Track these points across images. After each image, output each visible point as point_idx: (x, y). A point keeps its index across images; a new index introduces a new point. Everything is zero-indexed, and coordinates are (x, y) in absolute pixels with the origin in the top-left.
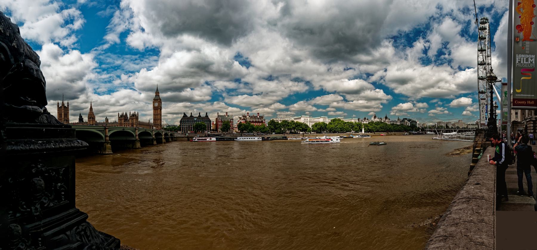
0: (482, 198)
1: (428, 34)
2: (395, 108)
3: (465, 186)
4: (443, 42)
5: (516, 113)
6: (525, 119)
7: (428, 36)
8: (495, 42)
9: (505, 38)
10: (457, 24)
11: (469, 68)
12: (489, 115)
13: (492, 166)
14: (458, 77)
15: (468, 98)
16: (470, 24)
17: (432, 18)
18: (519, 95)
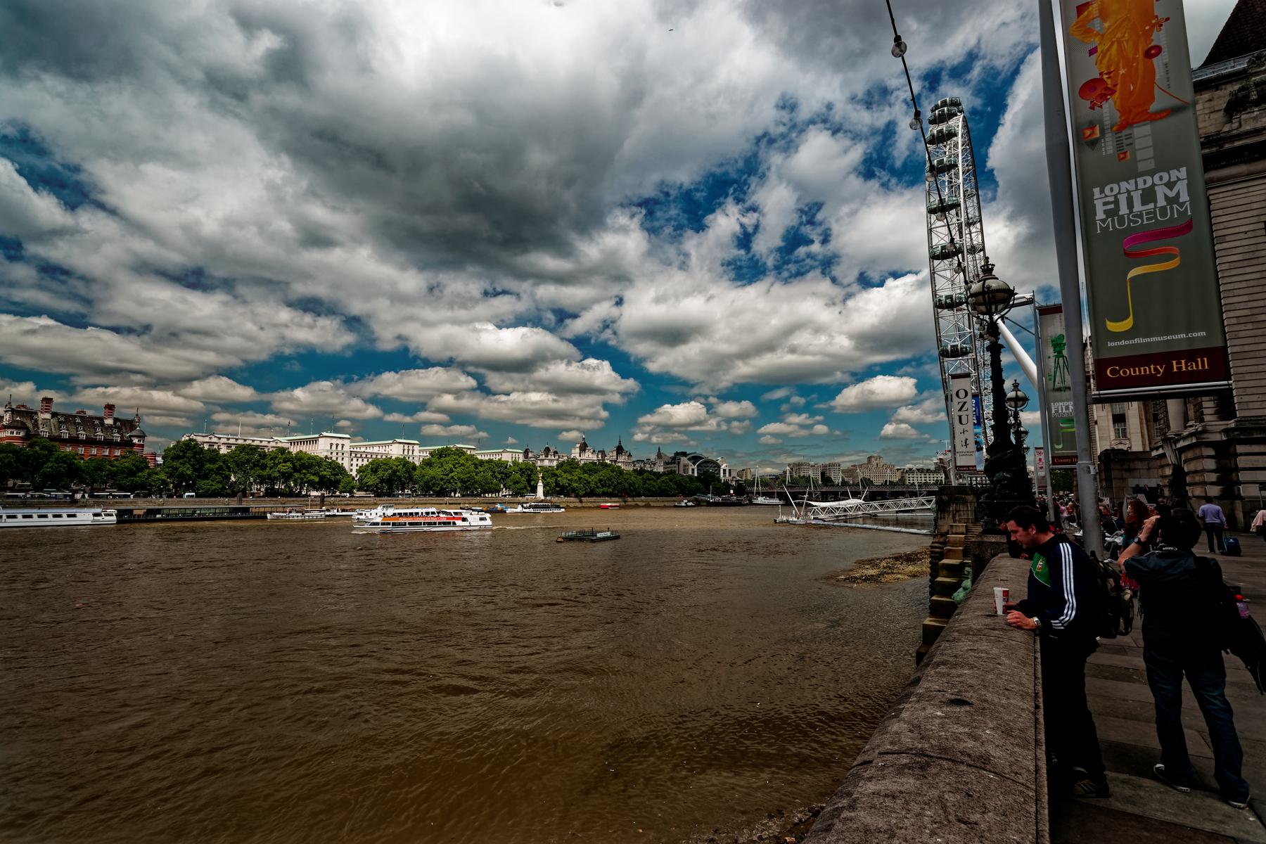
0: (983, 762)
1: (753, 187)
2: (648, 418)
3: (907, 706)
4: (803, 207)
5: (1119, 419)
6: (1167, 440)
7: (754, 192)
8: (992, 171)
9: (1037, 142)
10: (848, 142)
11: (896, 275)
12: (990, 432)
13: (1018, 635)
14: (857, 310)
15: (901, 376)
16: (895, 133)
17: (766, 139)
18: (1123, 343)
